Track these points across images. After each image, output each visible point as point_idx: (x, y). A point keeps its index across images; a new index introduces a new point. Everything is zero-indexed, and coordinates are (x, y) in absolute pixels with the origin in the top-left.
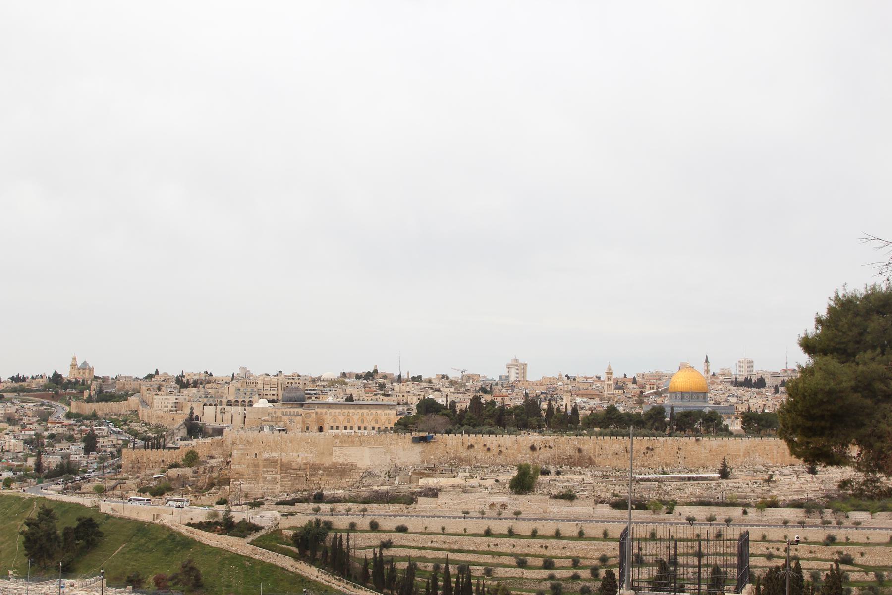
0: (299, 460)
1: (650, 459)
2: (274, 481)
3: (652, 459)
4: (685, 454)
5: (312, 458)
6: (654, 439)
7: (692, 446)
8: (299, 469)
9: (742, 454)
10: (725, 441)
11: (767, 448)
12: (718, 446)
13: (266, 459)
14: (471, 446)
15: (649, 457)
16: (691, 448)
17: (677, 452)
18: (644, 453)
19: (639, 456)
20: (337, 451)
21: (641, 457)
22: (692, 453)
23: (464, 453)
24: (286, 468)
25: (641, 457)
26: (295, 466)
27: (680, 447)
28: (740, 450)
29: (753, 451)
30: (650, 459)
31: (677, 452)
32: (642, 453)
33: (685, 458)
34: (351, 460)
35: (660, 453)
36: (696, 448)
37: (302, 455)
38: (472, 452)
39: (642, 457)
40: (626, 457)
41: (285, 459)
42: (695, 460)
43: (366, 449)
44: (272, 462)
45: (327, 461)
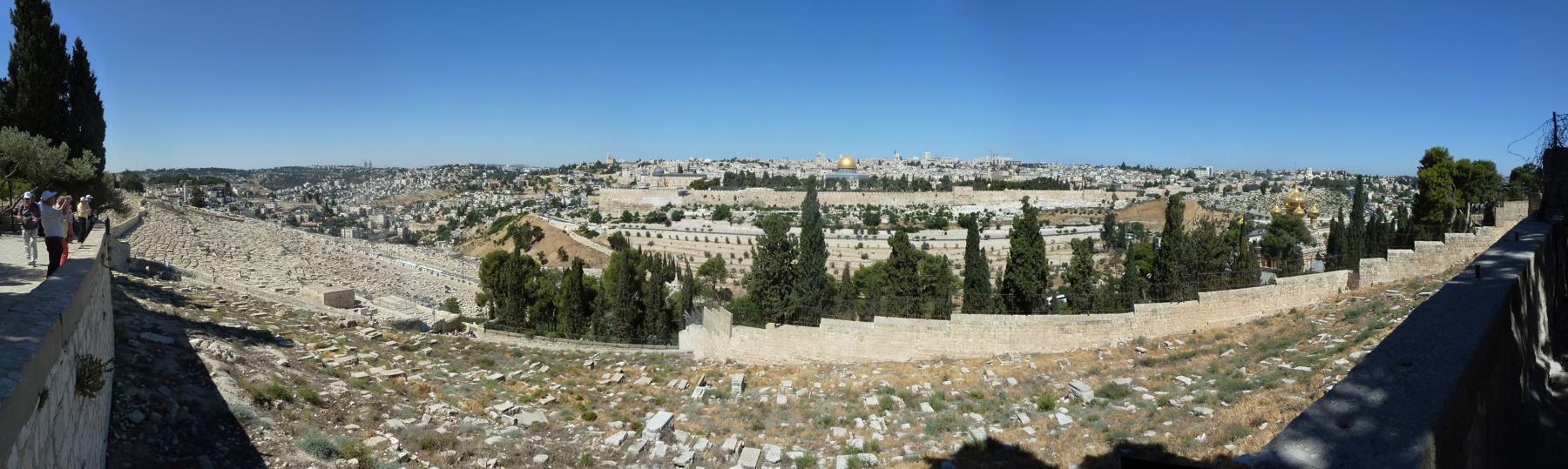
24: (622, 206)
37: (629, 199)
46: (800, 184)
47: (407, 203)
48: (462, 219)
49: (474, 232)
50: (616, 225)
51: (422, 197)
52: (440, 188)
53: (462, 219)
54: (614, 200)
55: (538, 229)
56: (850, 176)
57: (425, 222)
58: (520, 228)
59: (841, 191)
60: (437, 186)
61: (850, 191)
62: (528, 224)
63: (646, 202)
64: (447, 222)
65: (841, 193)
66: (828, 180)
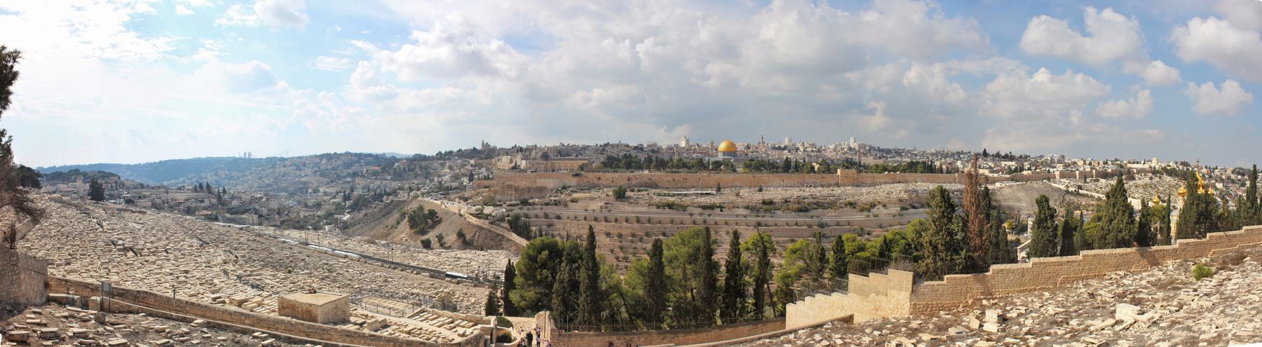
0: (523, 185)
2: (511, 195)
5: (528, 184)
8: (523, 189)
13: (508, 185)
14: (599, 178)
20: (538, 180)
23: (597, 182)
24: (517, 189)
26: (520, 188)
34: (545, 185)
38: (600, 181)
41: (516, 185)
43: (551, 180)
44: (510, 187)
45: (535, 186)
47: (291, 189)
48: (348, 203)
49: (362, 215)
50: (513, 208)
51: (305, 183)
52: (321, 176)
53: (348, 203)
54: (507, 183)
55: (432, 214)
57: (311, 207)
58: (414, 212)
60: (318, 173)
62: (421, 208)
63: (540, 185)
64: (334, 207)
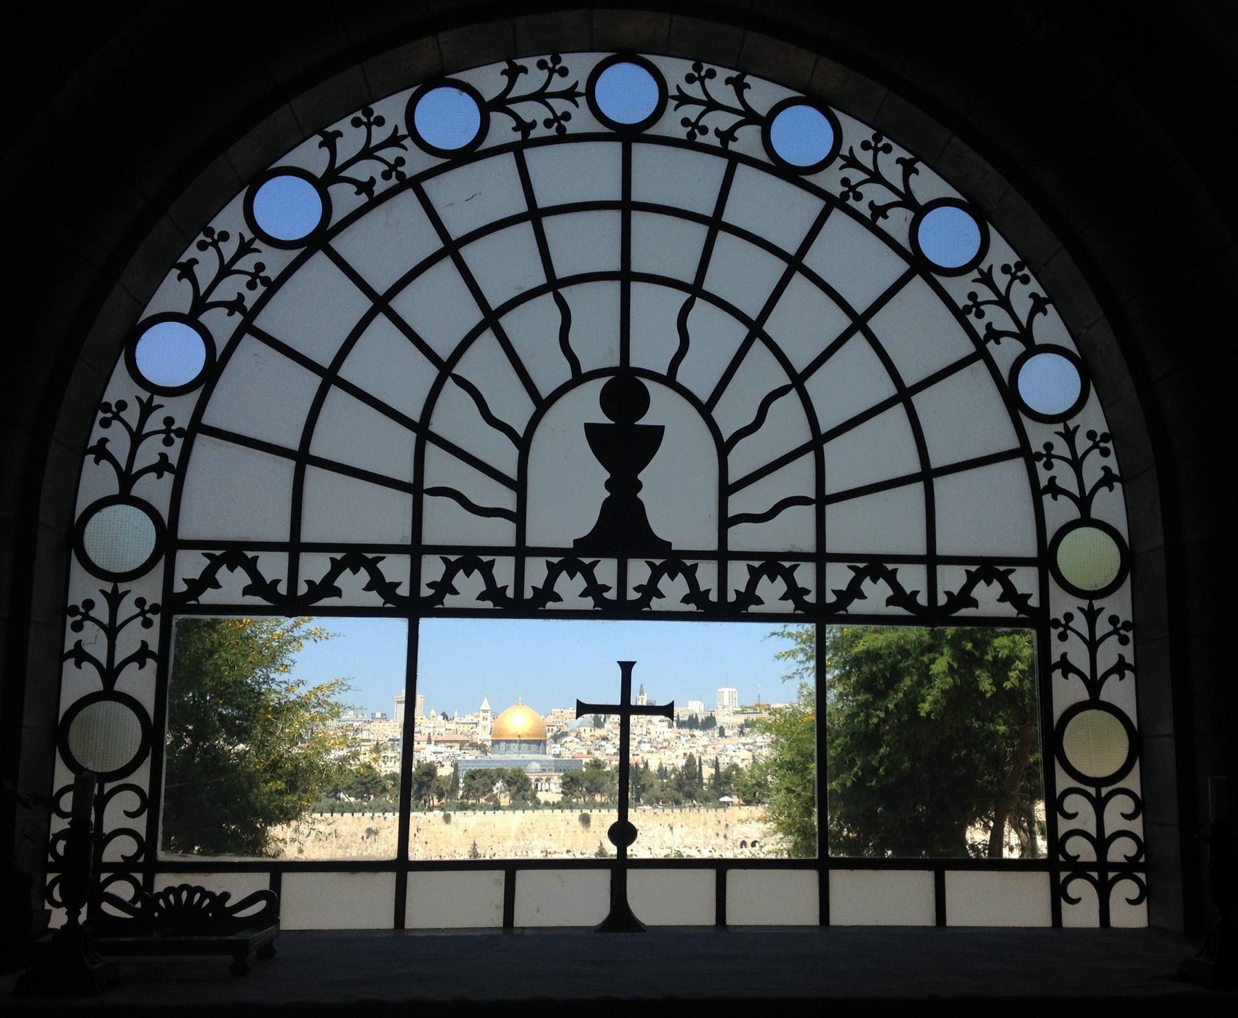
1: (372, 847)
3: (375, 846)
4: (426, 838)
6: (379, 817)
7: (438, 824)
9: (513, 834)
10: (488, 816)
11: (551, 825)
12: (479, 824)
15: (370, 844)
16: (438, 828)
17: (415, 835)
18: (363, 838)
19: (355, 843)
21: (357, 845)
22: (437, 836)
25: (357, 845)
27: (420, 827)
28: (510, 828)
29: (529, 829)
30: (372, 847)
31: (415, 835)
32: (360, 837)
33: (426, 843)
35: (387, 837)
36: (444, 827)
39: (360, 844)
40: (334, 844)
42: (441, 846)
46: (384, 790)
56: (532, 763)
59: (513, 807)
61: (537, 805)
65: (509, 813)
66: (472, 776)
